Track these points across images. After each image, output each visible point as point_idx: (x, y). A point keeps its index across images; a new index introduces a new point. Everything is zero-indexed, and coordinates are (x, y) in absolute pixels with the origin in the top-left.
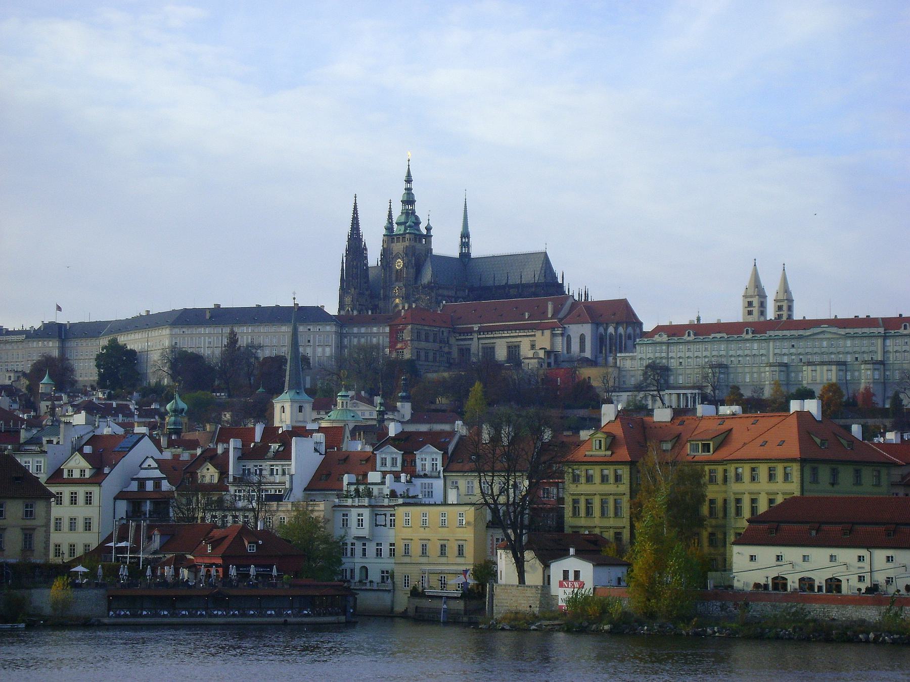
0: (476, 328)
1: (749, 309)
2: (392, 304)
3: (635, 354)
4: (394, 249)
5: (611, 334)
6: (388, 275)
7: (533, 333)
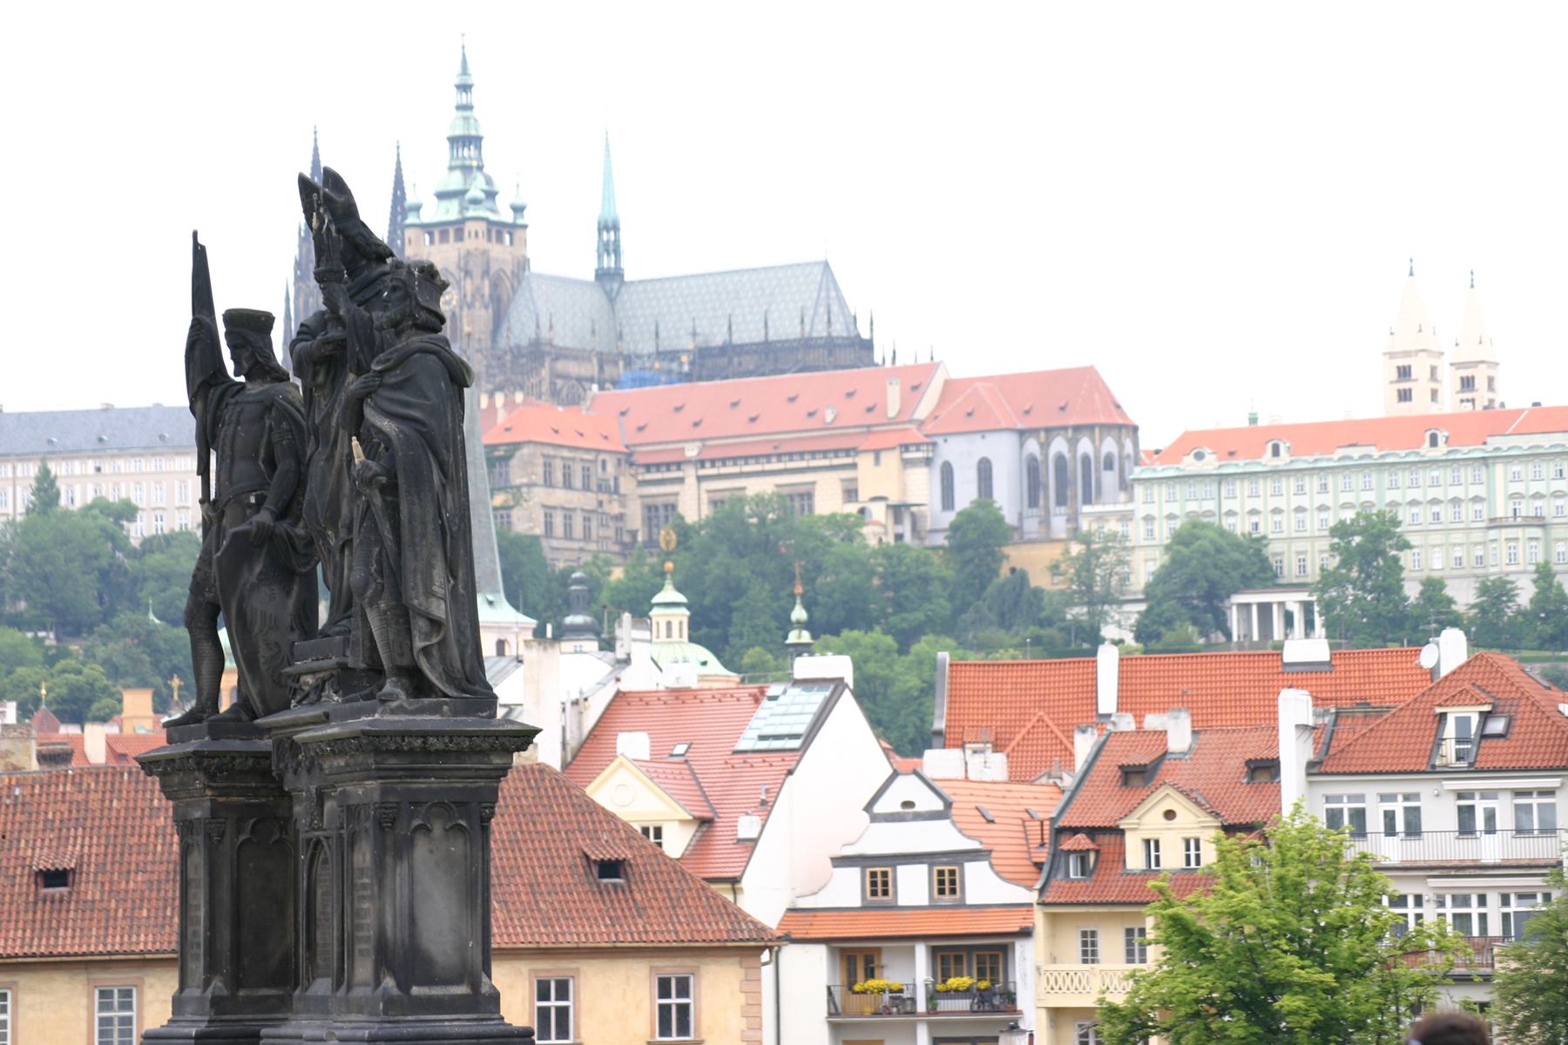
3: (1129, 507)
5: (1060, 459)
7: (848, 460)
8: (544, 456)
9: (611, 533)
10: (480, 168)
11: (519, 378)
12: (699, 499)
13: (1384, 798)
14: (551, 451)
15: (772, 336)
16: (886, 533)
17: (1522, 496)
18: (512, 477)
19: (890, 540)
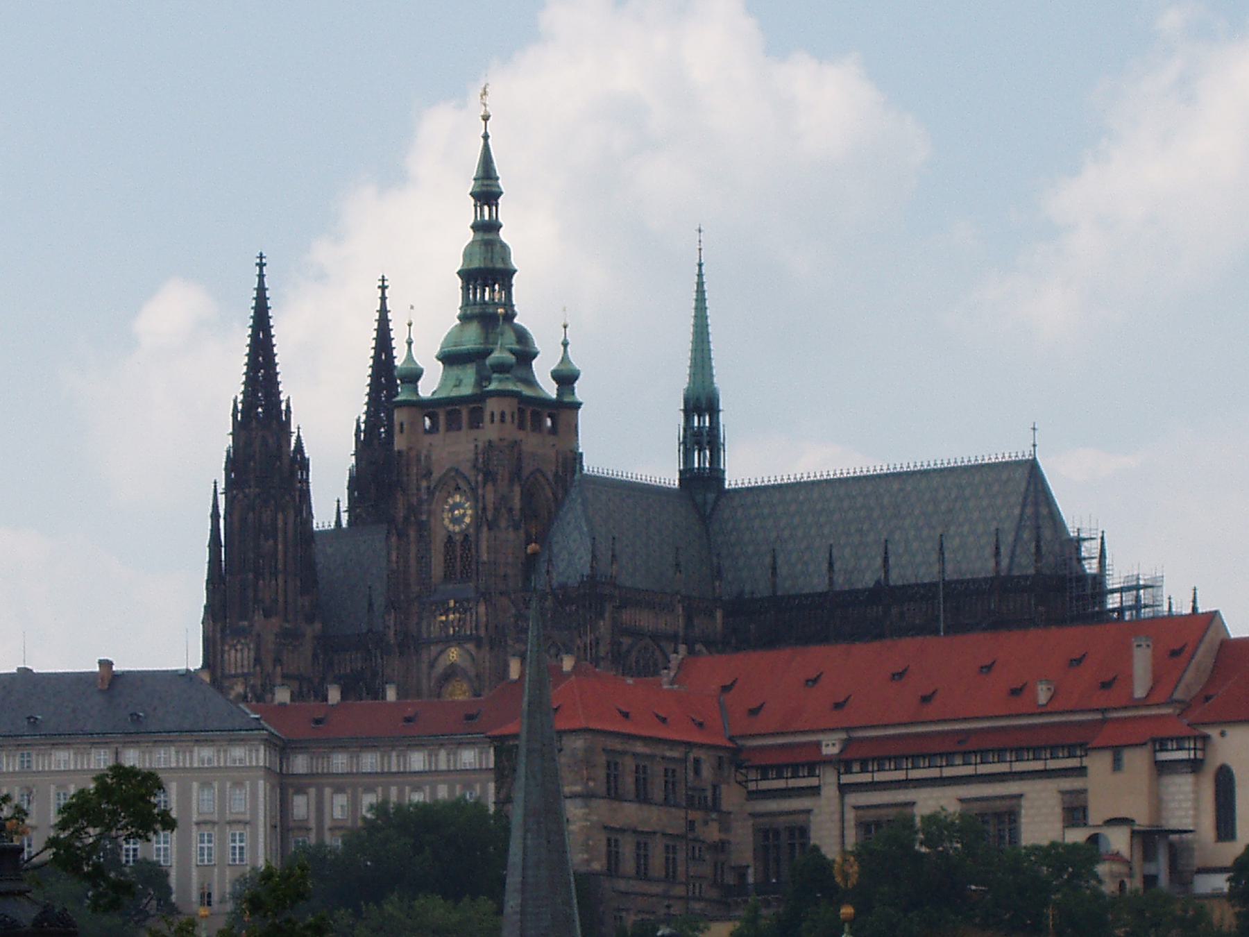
0: (831, 746)
2: (432, 665)
4: (434, 458)
6: (412, 555)
9: (707, 870)
10: (510, 316)
12: (842, 820)
14: (618, 745)
15: (950, 575)
16: (1131, 876)
19: (1135, 884)
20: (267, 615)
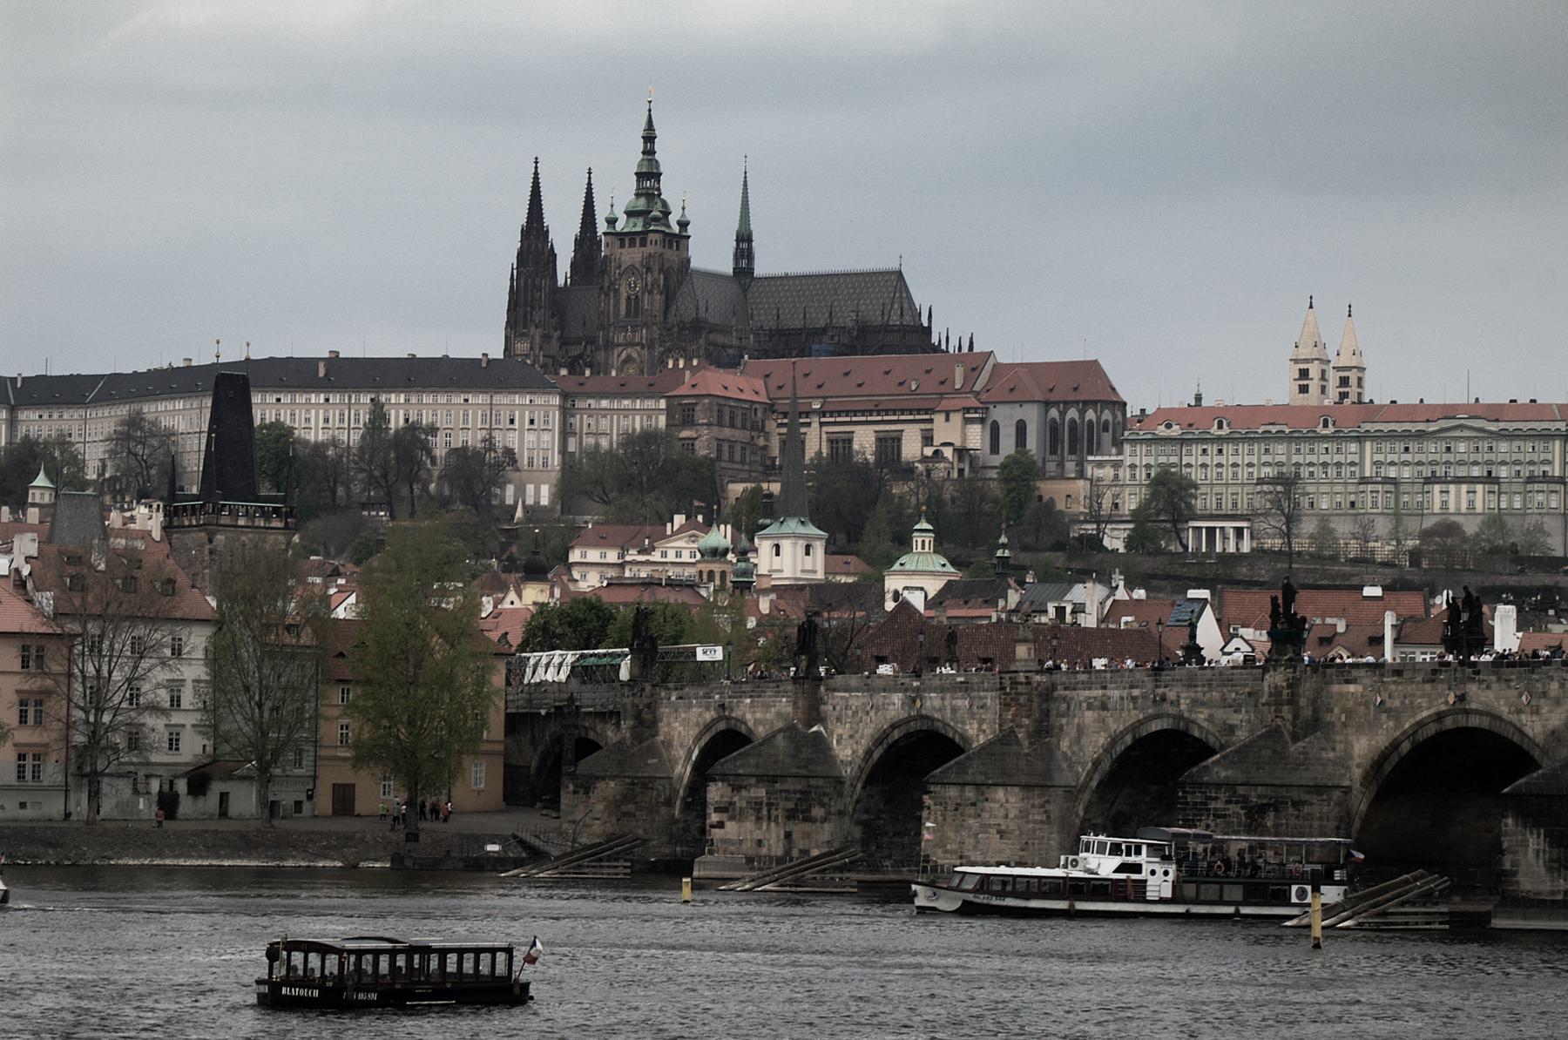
1: (1302, 382)
2: (619, 355)
3: (1120, 458)
5: (1073, 421)
7: (927, 417)
8: (718, 404)
9: (758, 458)
10: (660, 194)
11: (683, 344)
13: (1423, 653)
16: (953, 468)
17: (1382, 463)
18: (696, 418)
20: (537, 327)
